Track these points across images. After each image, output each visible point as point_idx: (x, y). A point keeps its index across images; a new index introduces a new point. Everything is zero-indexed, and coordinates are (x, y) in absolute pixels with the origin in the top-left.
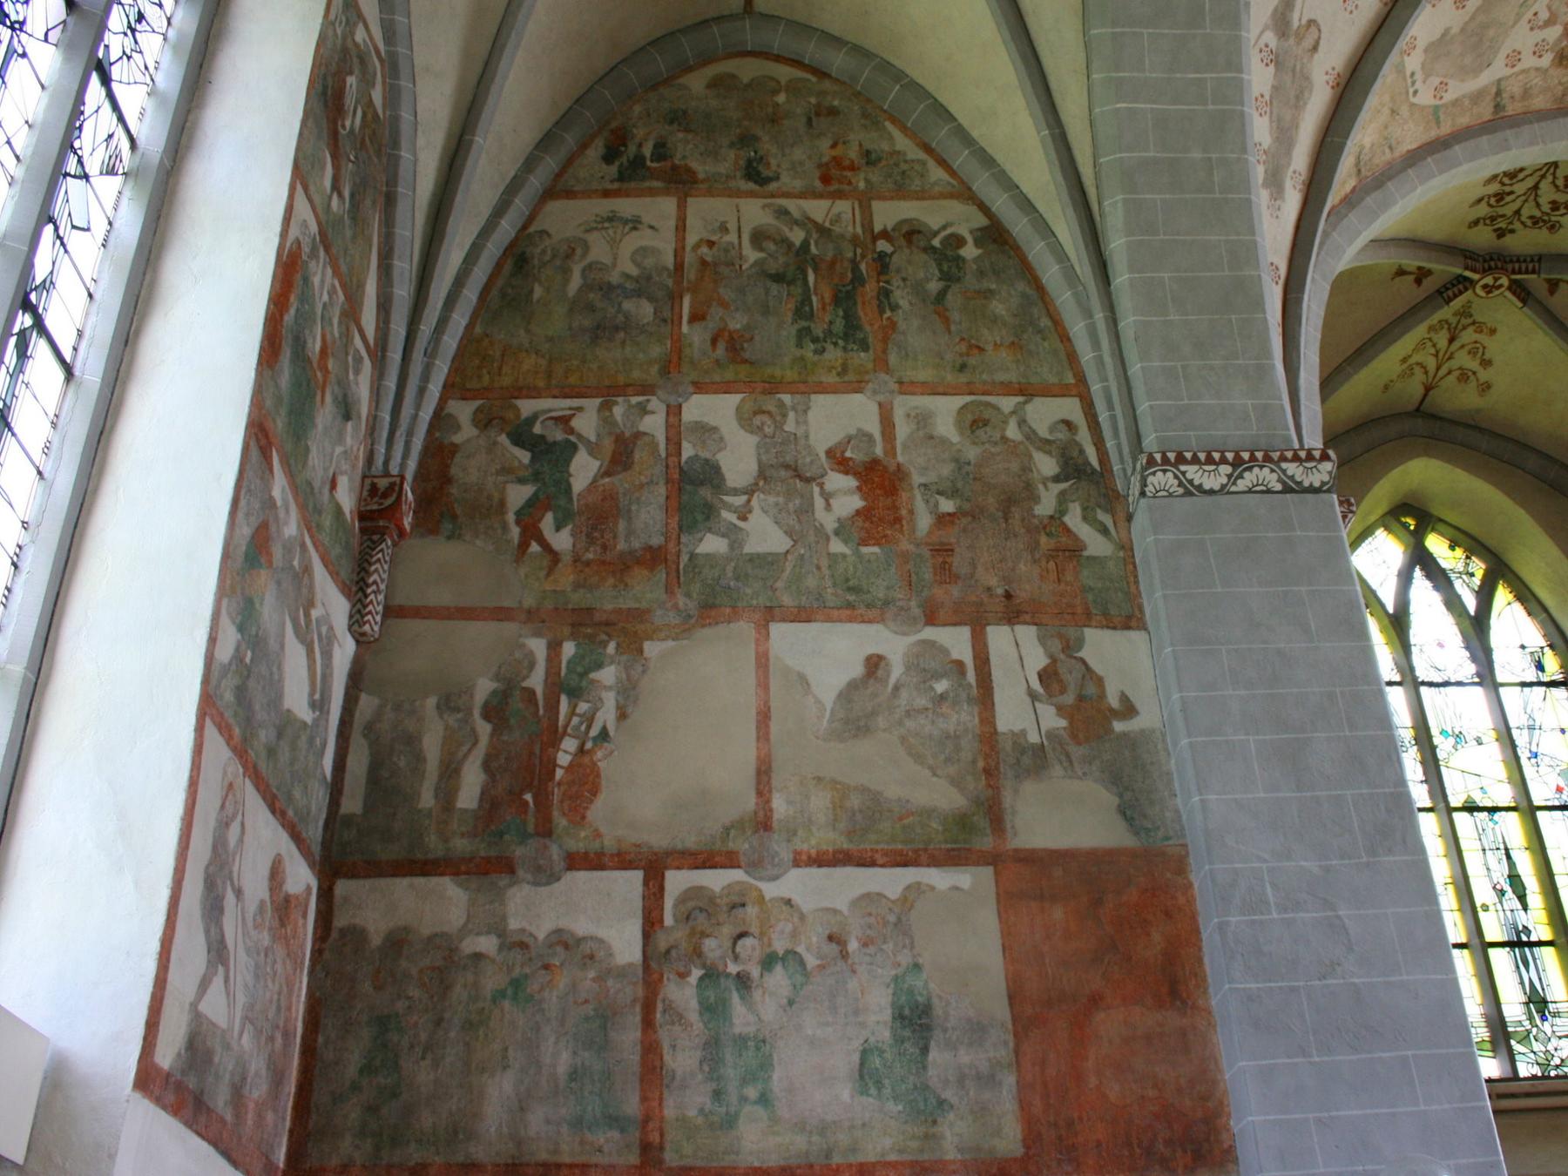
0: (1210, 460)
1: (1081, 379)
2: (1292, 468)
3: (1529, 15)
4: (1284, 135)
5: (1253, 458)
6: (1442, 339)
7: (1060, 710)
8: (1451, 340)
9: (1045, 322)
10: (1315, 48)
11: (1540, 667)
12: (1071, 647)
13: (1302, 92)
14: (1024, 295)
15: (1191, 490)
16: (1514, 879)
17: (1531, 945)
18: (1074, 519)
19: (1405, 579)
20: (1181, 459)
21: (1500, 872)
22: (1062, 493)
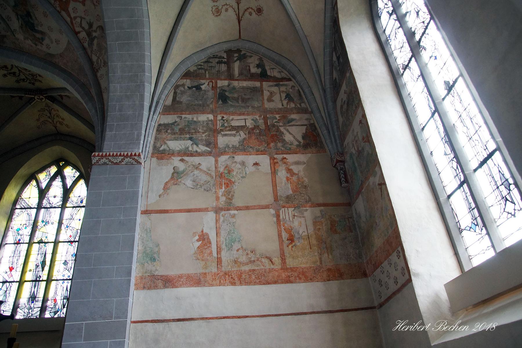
16: (44, 263)
19: (53, 178)
21: (40, 259)
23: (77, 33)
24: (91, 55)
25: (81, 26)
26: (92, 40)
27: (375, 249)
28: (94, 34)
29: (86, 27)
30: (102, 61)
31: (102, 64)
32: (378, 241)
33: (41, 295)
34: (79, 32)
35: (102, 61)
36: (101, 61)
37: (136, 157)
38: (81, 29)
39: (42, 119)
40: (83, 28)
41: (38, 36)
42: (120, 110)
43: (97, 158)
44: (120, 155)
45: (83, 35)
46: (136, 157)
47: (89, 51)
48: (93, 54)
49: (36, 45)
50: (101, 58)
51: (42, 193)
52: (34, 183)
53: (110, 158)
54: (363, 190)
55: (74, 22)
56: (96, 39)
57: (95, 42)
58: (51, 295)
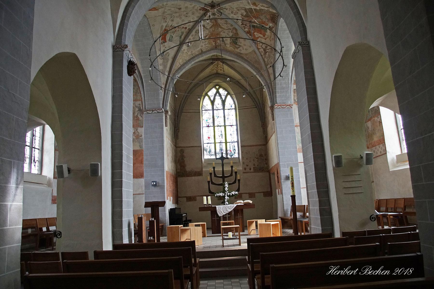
0: (150, 110)
1: (142, 99)
2: (158, 111)
3: (202, 42)
4: (165, 67)
5: (154, 110)
6: (216, 66)
7: (135, 136)
8: (217, 66)
9: (139, 91)
10: (169, 55)
11: (231, 107)
12: (137, 130)
13: (168, 61)
14: (137, 88)
15: (148, 113)
17: (222, 143)
18: (139, 116)
20: (147, 110)
22: (138, 113)
23: (258, 49)
24: (265, 59)
25: (261, 47)
26: (265, 53)
27: (374, 141)
28: (267, 51)
29: (264, 47)
30: (270, 62)
31: (270, 63)
32: (375, 139)
33: (224, 148)
34: (260, 49)
35: (270, 62)
36: (269, 61)
37: (291, 106)
38: (261, 48)
39: (213, 69)
40: (263, 48)
41: (237, 46)
42: (281, 85)
43: (277, 106)
44: (285, 105)
45: (262, 50)
46: (291, 106)
47: (264, 57)
48: (265, 58)
49: (235, 49)
50: (269, 60)
51: (213, 102)
52: (207, 97)
53: (282, 106)
54: (372, 120)
55: (258, 45)
56: (268, 53)
57: (267, 54)
58: (228, 148)
